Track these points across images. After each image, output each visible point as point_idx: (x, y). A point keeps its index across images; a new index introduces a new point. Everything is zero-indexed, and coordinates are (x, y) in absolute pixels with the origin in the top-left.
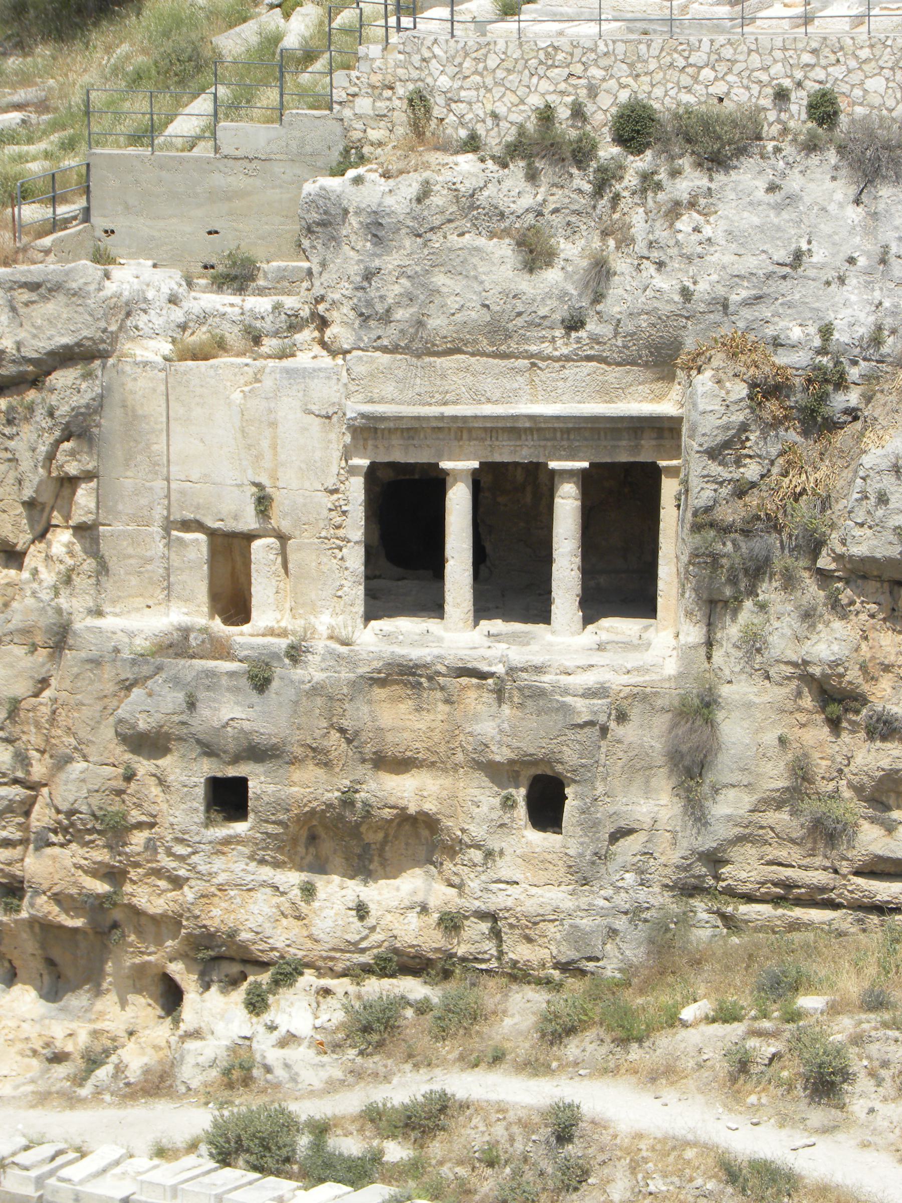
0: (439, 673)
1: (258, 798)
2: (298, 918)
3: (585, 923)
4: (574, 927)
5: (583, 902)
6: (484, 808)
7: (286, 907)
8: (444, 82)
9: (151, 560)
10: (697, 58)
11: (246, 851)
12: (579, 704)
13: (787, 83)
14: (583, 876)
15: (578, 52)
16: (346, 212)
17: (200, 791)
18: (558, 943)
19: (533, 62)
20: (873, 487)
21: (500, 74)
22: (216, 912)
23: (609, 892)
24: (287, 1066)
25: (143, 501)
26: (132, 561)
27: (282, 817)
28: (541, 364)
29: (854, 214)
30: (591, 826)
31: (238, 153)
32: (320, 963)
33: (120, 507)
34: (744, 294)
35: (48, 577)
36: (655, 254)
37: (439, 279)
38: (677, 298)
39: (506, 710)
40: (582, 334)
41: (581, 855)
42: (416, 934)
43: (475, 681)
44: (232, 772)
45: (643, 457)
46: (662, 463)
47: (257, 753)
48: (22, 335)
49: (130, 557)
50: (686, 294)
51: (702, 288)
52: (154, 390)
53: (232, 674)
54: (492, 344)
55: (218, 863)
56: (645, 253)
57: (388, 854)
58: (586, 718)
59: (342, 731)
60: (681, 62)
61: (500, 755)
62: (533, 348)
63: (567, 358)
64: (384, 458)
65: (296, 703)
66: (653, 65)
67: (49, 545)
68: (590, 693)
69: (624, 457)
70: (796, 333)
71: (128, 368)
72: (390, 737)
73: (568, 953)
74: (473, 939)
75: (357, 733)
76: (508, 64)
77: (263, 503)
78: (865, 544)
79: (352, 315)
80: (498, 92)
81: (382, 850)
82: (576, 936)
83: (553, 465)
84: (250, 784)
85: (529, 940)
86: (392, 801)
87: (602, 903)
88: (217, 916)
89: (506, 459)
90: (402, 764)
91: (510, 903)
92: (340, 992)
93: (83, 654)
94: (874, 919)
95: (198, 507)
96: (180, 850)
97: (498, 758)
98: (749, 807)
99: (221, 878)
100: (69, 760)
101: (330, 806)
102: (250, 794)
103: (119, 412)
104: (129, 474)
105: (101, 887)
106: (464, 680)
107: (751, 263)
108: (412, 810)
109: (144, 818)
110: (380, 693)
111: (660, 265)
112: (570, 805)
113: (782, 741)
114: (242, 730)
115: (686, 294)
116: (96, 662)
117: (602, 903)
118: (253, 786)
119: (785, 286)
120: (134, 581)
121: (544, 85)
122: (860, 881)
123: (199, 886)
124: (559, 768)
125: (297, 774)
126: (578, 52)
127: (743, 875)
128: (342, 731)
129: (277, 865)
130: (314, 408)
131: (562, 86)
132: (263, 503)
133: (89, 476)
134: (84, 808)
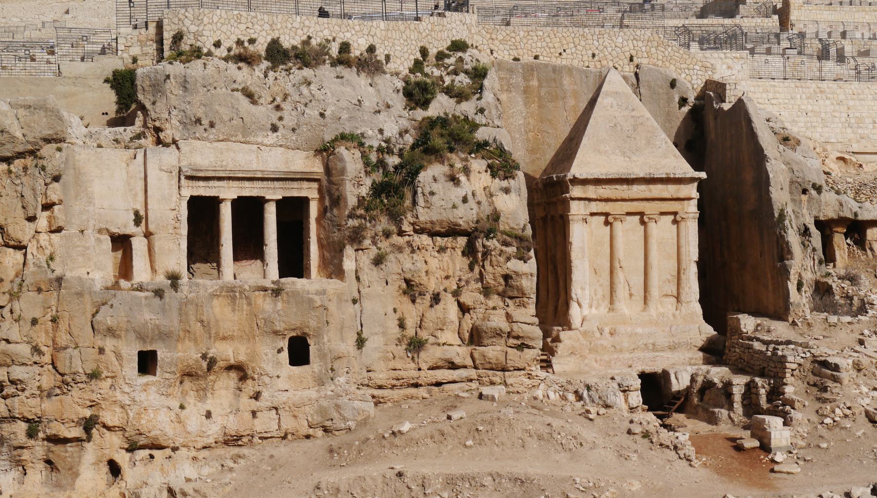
0: (245, 290)
1: (163, 359)
2: (180, 422)
3: (325, 403)
4: (320, 406)
5: (322, 394)
6: (270, 355)
7: (173, 417)
8: (193, 28)
9: (88, 248)
10: (296, 25)
11: (155, 389)
12: (317, 298)
13: (330, 38)
14: (320, 382)
15: (250, 18)
16: (168, 77)
17: (136, 358)
18: (312, 415)
19: (232, 21)
20: (427, 192)
21: (219, 25)
22: (143, 422)
23: (333, 387)
24: (196, 491)
25: (84, 217)
26: (80, 249)
27: (173, 369)
28: (262, 148)
29: (370, 89)
30: (322, 356)
31: (71, 76)
32: (190, 444)
33: (73, 221)
34: (346, 116)
35: (43, 259)
36: (303, 101)
37: (218, 108)
38: (319, 117)
39: (280, 305)
40: (278, 134)
41: (320, 371)
42: (233, 425)
43: (262, 293)
44: (149, 348)
45: (303, 194)
46: (310, 197)
47: (164, 336)
48: (24, 131)
49: (79, 246)
50: (322, 115)
51: (327, 113)
52: (89, 160)
53: (146, 298)
54: (243, 137)
55: (143, 396)
56: (298, 99)
57: (216, 387)
58: (319, 303)
59: (202, 322)
60: (290, 26)
61: (280, 326)
62: (259, 140)
63: (271, 146)
64: (196, 193)
65: (180, 309)
66: (279, 26)
67: (38, 242)
68: (318, 293)
69: (295, 194)
70: (370, 132)
71: (76, 149)
72: (221, 324)
73: (317, 419)
74: (266, 422)
75: (209, 323)
76: (222, 21)
78: (424, 216)
79: (178, 124)
80: (218, 33)
81: (213, 386)
82: (322, 411)
83: (267, 197)
84: (158, 353)
85: (295, 416)
86: (224, 357)
87: (330, 393)
88: (144, 424)
89: (248, 194)
90: (224, 338)
91: (285, 399)
92: (200, 457)
93: (73, 290)
94: (436, 389)
95: (107, 222)
96: (127, 389)
97: (278, 328)
98: (383, 343)
99: (146, 404)
100: (65, 348)
101: (197, 361)
102: (159, 358)
103: (72, 172)
104: (77, 203)
105: (88, 413)
106: (257, 293)
107: (344, 103)
108: (232, 362)
109: (109, 374)
110: (215, 302)
111: (306, 105)
112: (312, 349)
113: (395, 311)
114: (155, 324)
115: (322, 115)
116: (80, 294)
117: (330, 393)
118: (160, 355)
119: (359, 114)
120: (80, 259)
121: (237, 32)
122: (431, 372)
123: (135, 408)
124: (307, 330)
125: (180, 346)
126: (250, 18)
127: (381, 376)
128: (202, 322)
129: (168, 395)
130: (164, 168)
131: (244, 32)
132: (138, 220)
133: (61, 202)
134: (81, 370)
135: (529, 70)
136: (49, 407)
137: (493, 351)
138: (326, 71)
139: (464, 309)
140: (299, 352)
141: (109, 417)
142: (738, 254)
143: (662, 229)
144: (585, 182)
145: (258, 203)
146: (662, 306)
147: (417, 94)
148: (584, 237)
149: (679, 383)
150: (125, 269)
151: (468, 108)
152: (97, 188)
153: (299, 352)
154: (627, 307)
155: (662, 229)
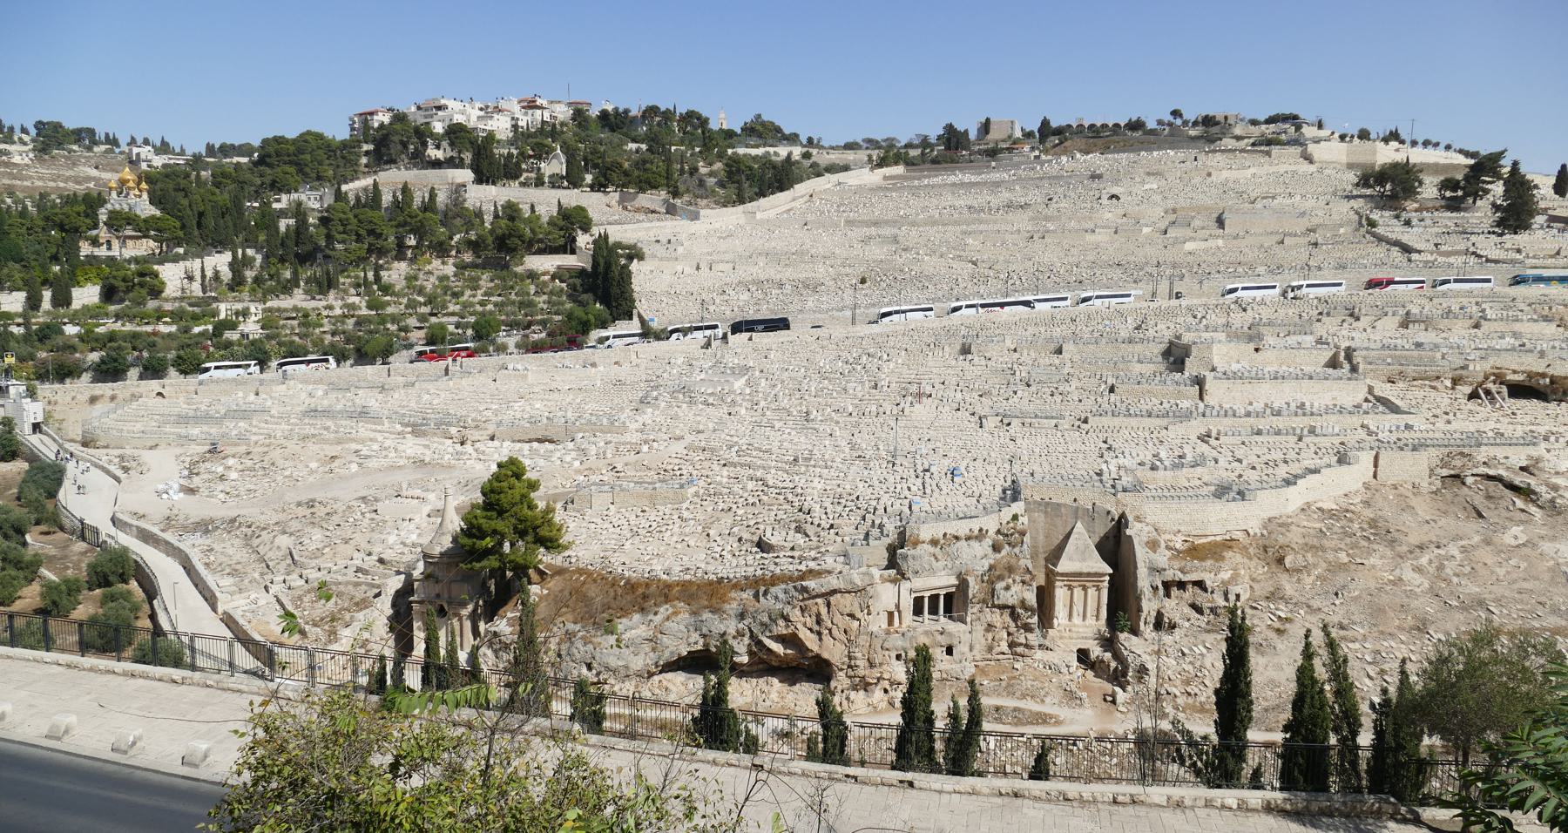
77: (898, 606)
135: (1048, 504)
136: (867, 672)
137: (1020, 650)
138: (963, 543)
139: (1009, 634)
140: (950, 651)
141: (886, 676)
142: (1122, 606)
143: (1092, 592)
144: (1062, 575)
145: (937, 596)
146: (1091, 621)
147: (996, 548)
148: (1061, 594)
149: (1093, 656)
150: (890, 623)
151: (1017, 550)
152: (884, 598)
153: (950, 651)
154: (1077, 620)
155: (1092, 592)
